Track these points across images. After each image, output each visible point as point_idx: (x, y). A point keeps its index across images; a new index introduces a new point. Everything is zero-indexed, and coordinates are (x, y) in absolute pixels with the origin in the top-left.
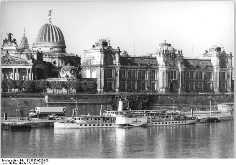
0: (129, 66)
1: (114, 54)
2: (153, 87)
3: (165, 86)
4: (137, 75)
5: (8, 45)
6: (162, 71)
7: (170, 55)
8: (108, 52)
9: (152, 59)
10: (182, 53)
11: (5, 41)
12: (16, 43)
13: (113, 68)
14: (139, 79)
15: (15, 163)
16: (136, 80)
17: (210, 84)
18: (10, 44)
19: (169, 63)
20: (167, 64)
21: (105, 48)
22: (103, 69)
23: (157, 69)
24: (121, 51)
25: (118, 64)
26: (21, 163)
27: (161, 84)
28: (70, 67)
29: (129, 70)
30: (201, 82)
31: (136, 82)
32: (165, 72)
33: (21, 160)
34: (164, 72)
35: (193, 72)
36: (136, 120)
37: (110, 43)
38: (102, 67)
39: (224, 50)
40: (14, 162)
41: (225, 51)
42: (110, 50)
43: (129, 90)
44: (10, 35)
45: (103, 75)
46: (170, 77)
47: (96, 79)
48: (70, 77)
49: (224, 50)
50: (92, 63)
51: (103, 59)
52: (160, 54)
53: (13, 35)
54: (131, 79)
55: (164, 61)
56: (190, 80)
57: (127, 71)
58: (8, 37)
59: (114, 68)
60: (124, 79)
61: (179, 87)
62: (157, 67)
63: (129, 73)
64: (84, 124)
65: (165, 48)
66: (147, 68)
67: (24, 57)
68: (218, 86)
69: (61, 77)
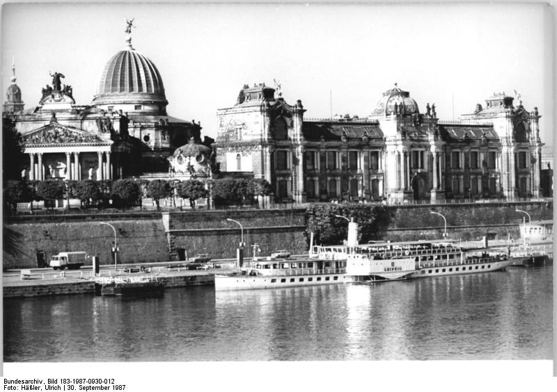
0: (322, 143)
1: (290, 115)
2: (375, 190)
3: (403, 186)
7: (409, 117)
8: (278, 114)
9: (370, 126)
10: (436, 111)
11: (47, 92)
12: (70, 95)
13: (288, 147)
16: (337, 175)
17: (495, 179)
18: (58, 99)
19: (408, 134)
20: (405, 136)
21: (272, 103)
22: (268, 149)
23: (383, 147)
25: (299, 138)
28: (195, 148)
30: (477, 174)
31: (339, 178)
32: (402, 155)
34: (399, 155)
35: (458, 153)
36: (393, 264)
37: (281, 91)
38: (266, 147)
39: (521, 102)
41: (523, 104)
42: (281, 108)
43: (324, 197)
44: (57, 78)
45: (268, 163)
46: (412, 166)
47: (252, 172)
48: (196, 170)
49: (521, 102)
50: (241, 136)
51: (267, 127)
52: (387, 115)
53: (64, 77)
54: (328, 171)
55: (398, 130)
56: (453, 170)
57: (340, 154)
58: (53, 83)
59: (292, 147)
60: (313, 172)
61: (432, 188)
62: (382, 143)
63: (323, 159)
64: (281, 278)
65: (398, 100)
66: (360, 147)
67: (91, 127)
68: (513, 184)
69: (176, 170)
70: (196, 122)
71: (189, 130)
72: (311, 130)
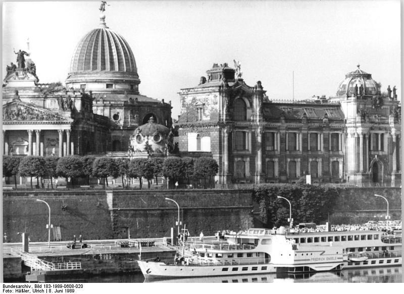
0: (282, 124)
1: (250, 96)
2: (336, 172)
3: (361, 169)
4: (299, 145)
5: (17, 78)
6: (354, 134)
7: (369, 99)
9: (331, 108)
11: (11, 69)
12: (34, 74)
14: (305, 154)
15: (26, 291)
16: (297, 156)
18: (22, 76)
19: (368, 116)
20: (364, 119)
21: (231, 84)
22: (225, 131)
23: (344, 129)
24: (264, 89)
26: (36, 291)
27: (351, 165)
28: (154, 127)
29: (283, 134)
31: (299, 160)
32: (361, 137)
33: (36, 286)
34: (359, 138)
37: (241, 72)
38: (224, 127)
40: (24, 289)
43: (283, 178)
44: (21, 55)
46: (372, 148)
47: (211, 152)
48: (154, 149)
50: (201, 117)
51: (225, 108)
52: (348, 97)
55: (358, 112)
58: (18, 61)
59: (249, 127)
60: (272, 153)
62: (343, 125)
63: (283, 141)
65: (358, 83)
66: (320, 129)
67: (52, 105)
69: (135, 149)
70: (166, 101)
71: (159, 109)
72: (271, 111)
